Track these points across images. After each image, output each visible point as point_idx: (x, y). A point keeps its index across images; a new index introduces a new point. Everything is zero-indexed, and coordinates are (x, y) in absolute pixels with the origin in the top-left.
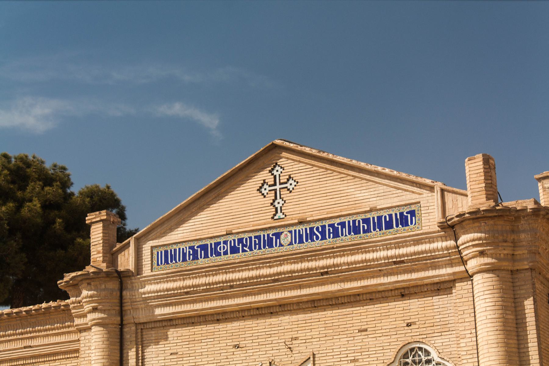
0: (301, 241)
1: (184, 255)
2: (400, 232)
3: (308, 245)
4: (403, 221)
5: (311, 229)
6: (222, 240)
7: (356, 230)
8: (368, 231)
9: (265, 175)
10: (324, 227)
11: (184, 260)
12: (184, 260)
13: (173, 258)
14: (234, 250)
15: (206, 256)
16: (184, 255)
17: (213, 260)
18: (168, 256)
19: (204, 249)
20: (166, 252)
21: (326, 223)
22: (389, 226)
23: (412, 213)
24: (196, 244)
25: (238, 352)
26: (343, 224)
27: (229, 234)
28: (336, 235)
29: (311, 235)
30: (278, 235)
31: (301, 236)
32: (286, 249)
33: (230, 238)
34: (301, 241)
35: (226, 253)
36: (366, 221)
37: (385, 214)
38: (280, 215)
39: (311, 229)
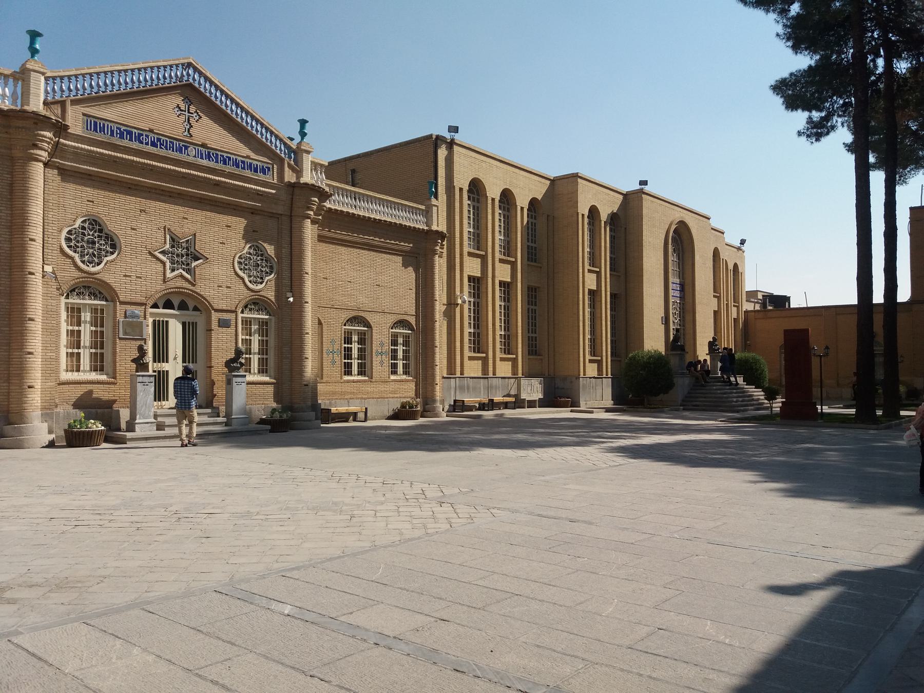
1: (112, 132)
2: (261, 177)
3: (205, 162)
4: (263, 171)
5: (209, 153)
6: (144, 133)
8: (244, 168)
11: (112, 135)
12: (112, 135)
13: (102, 130)
14: (154, 144)
15: (131, 140)
16: (112, 132)
17: (135, 145)
19: (127, 132)
20: (95, 123)
21: (219, 153)
24: (123, 128)
26: (229, 158)
27: (151, 131)
29: (209, 157)
30: (186, 148)
31: (202, 154)
32: (190, 159)
33: (151, 135)
34: (202, 158)
35: (147, 144)
36: (243, 162)
37: (255, 162)
39: (209, 153)
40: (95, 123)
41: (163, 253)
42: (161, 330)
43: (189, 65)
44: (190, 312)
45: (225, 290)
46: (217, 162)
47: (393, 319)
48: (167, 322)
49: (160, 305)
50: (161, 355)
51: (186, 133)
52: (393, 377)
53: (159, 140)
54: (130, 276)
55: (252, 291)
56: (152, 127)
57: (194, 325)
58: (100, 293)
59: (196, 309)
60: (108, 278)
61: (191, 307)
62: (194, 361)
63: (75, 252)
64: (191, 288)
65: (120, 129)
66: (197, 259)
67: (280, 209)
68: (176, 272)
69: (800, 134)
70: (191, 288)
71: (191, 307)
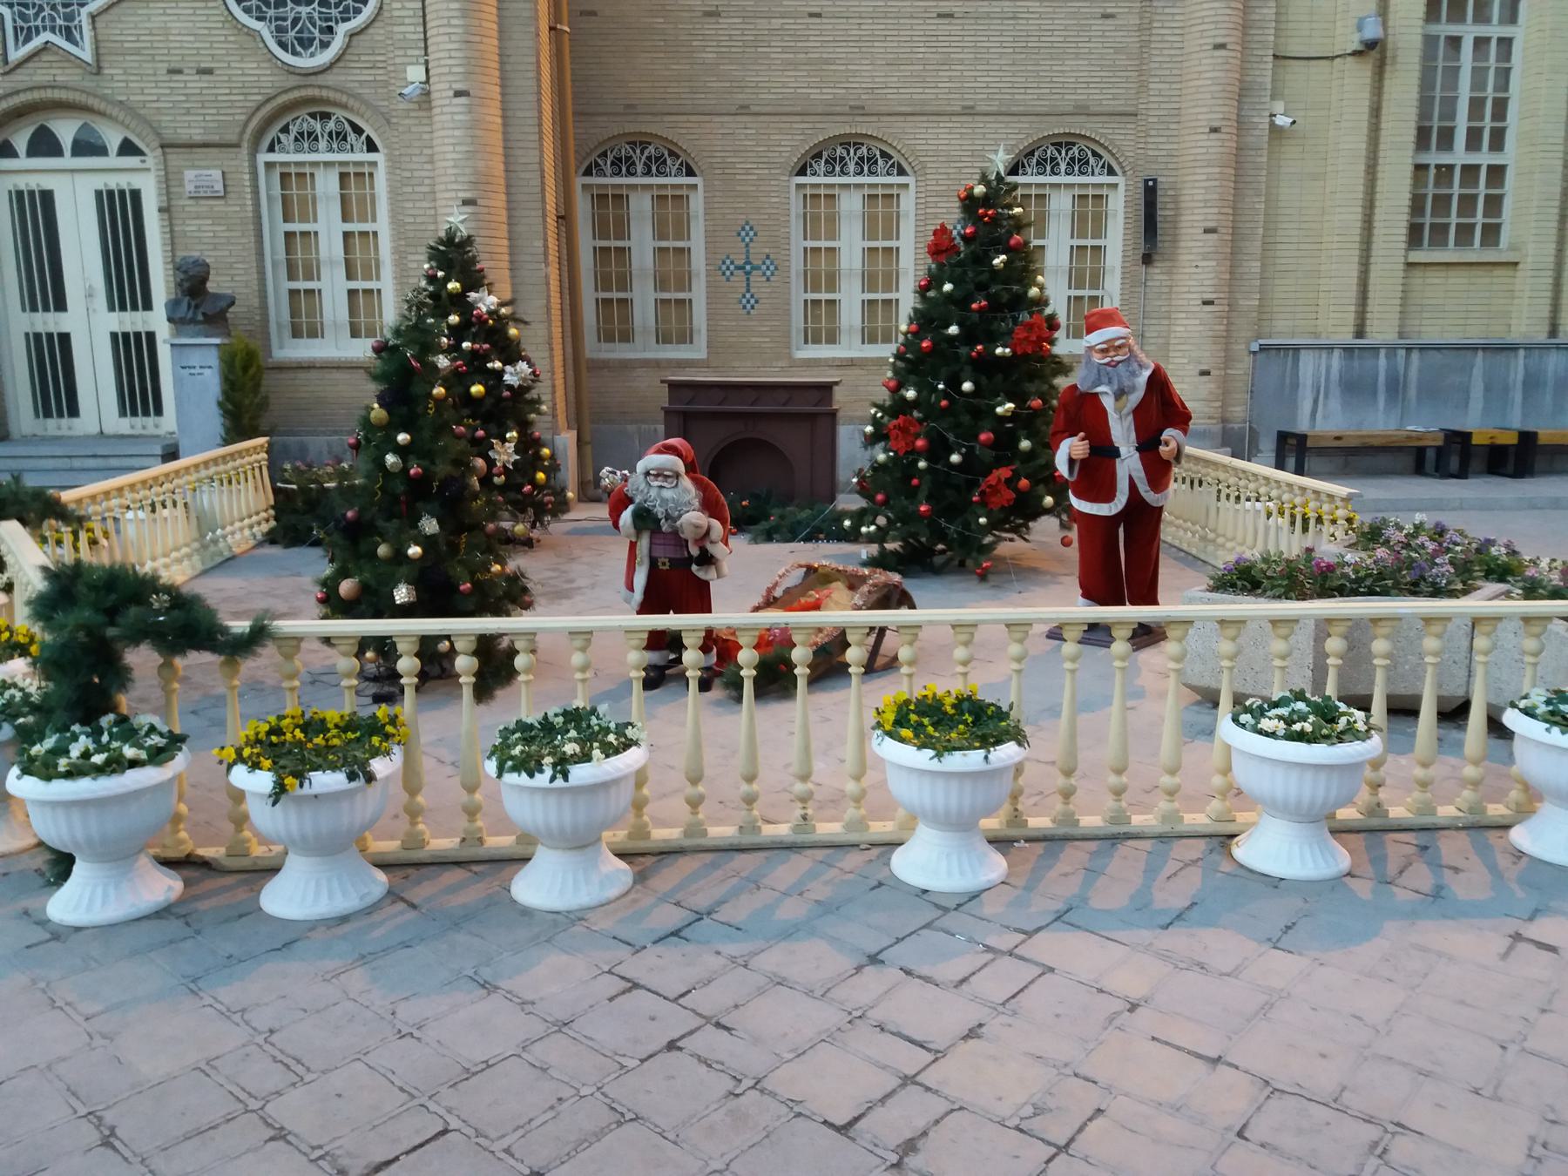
44: (112, 160)
48: (47, 197)
55: (291, 70)
59: (128, 148)
64: (88, 84)
68: (37, 42)
70: (88, 84)
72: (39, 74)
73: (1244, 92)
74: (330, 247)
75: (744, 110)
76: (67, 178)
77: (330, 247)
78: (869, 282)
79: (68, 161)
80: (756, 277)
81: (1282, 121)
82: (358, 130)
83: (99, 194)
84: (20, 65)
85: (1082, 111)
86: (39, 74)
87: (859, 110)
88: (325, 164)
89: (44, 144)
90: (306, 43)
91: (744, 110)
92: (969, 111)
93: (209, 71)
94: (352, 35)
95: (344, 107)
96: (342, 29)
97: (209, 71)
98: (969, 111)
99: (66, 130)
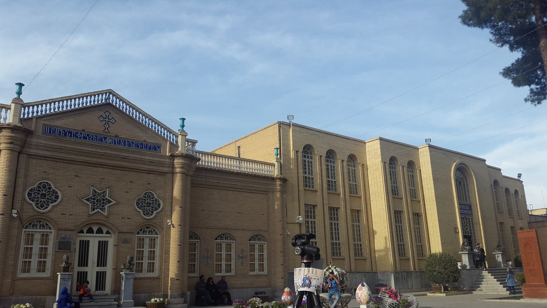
0: (115, 143)
1: (60, 132)
4: (155, 148)
5: (120, 140)
7: (138, 147)
8: (142, 148)
9: (102, 113)
10: (125, 141)
14: (85, 138)
16: (60, 132)
18: (50, 131)
20: (50, 129)
22: (150, 149)
23: (159, 147)
25: (77, 178)
28: (130, 146)
29: (119, 143)
30: (105, 138)
31: (115, 142)
33: (83, 133)
35: (80, 138)
36: (142, 144)
38: (106, 130)
39: (120, 140)
40: (50, 129)
41: (88, 200)
42: (85, 245)
43: (111, 92)
44: (104, 235)
45: (127, 220)
46: (125, 145)
47: (249, 235)
48: (88, 241)
49: (85, 231)
50: (83, 261)
51: (106, 130)
52: (252, 273)
53: (88, 135)
54: (65, 214)
55: (145, 219)
56: (84, 128)
57: (106, 243)
58: (47, 224)
59: (108, 232)
60: (51, 215)
61: (105, 232)
62: (105, 265)
63: (33, 201)
65: (64, 131)
66: (109, 202)
67: (166, 169)
68: (96, 211)
69: (526, 100)
71: (105, 232)
72: (96, 217)
73: (283, 228)
74: (146, 254)
75: (207, 228)
76: (93, 238)
77: (257, 256)
78: (150, 258)
79: (95, 235)
80: (244, 259)
81: (289, 233)
82: (154, 231)
83: (99, 242)
84: (92, 215)
85: (260, 230)
86: (96, 217)
87: (226, 228)
88: (147, 237)
89: (90, 231)
90: (148, 214)
91: (207, 228)
92: (243, 229)
93: (130, 218)
94: (157, 213)
95: (154, 226)
96: (155, 212)
97: (130, 218)
98: (243, 229)
99: (95, 229)
